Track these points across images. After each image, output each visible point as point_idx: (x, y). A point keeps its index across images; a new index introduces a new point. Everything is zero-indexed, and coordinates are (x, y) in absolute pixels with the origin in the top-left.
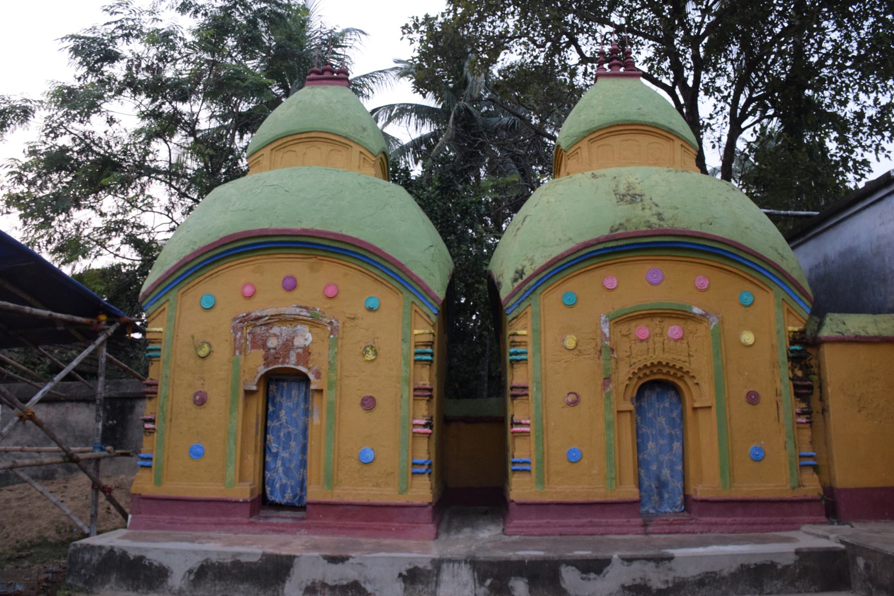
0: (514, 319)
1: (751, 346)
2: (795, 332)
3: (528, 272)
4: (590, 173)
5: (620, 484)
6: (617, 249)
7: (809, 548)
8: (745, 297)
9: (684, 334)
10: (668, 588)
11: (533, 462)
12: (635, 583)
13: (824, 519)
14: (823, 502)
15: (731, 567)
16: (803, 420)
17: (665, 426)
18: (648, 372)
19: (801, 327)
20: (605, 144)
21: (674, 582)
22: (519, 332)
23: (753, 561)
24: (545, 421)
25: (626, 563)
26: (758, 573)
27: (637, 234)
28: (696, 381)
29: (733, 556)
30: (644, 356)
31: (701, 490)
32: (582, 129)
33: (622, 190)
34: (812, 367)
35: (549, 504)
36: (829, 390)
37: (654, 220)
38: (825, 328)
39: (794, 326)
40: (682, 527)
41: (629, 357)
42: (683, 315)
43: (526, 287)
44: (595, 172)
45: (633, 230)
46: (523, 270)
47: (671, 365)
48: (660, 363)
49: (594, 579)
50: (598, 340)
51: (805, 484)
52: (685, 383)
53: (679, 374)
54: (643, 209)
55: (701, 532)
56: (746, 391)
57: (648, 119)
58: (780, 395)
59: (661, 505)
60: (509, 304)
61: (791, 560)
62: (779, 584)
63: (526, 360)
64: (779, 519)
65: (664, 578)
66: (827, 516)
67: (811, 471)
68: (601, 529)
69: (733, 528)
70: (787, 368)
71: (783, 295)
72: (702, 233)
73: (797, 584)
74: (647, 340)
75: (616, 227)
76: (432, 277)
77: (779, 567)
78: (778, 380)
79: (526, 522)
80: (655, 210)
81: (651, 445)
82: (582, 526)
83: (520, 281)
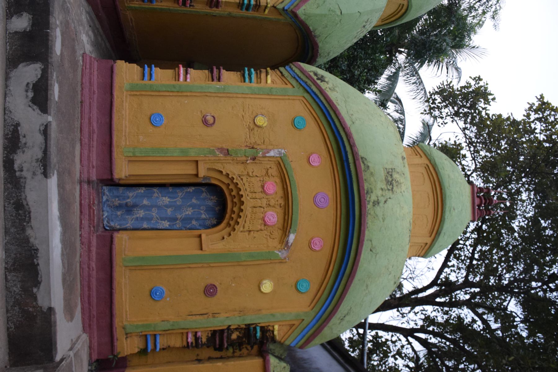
0: (281, 73)
1: (260, 290)
2: (273, 332)
3: (323, 85)
4: (405, 156)
5: (130, 161)
6: (345, 164)
7: (55, 322)
8: (304, 285)
9: (268, 225)
10: (15, 171)
11: (150, 82)
12: (21, 137)
13: (95, 357)
14: (111, 357)
15: (35, 239)
16: (191, 339)
17: (184, 214)
18: (234, 193)
19: (278, 338)
20: (424, 179)
21: (21, 178)
22: (269, 77)
23: (41, 262)
24: (189, 94)
25: (42, 128)
26: (26, 265)
27: (360, 181)
28: (225, 237)
29: (47, 241)
30: (249, 188)
31: (121, 239)
32: (436, 159)
33: (395, 176)
34: (240, 350)
35: (112, 94)
36: (220, 364)
37: (373, 198)
38: (277, 361)
39: (279, 330)
40: (87, 217)
41: (248, 175)
42: (287, 224)
43: (309, 82)
44: (406, 160)
45: (364, 178)
46: (324, 81)
47: (241, 214)
48: (242, 203)
49: (27, 96)
50: (263, 147)
51: (129, 340)
52: (223, 229)
53: (232, 223)
54: (382, 189)
55: (81, 235)
56: (217, 284)
57: (447, 215)
58: (214, 317)
59: (109, 206)
60: (294, 68)
61: (42, 302)
62: (17, 289)
63: (245, 82)
64: (95, 313)
65: (26, 166)
66: (97, 361)
67: (142, 346)
68: (86, 140)
69: (85, 267)
70: (239, 324)
71: (307, 320)
72: (363, 240)
73: (17, 308)
74: (264, 191)
75: (365, 162)
76: (316, 6)
77: (35, 290)
78: (228, 313)
79: (96, 73)
80: (382, 200)
81: (166, 200)
82: (90, 123)
83: (315, 78)
